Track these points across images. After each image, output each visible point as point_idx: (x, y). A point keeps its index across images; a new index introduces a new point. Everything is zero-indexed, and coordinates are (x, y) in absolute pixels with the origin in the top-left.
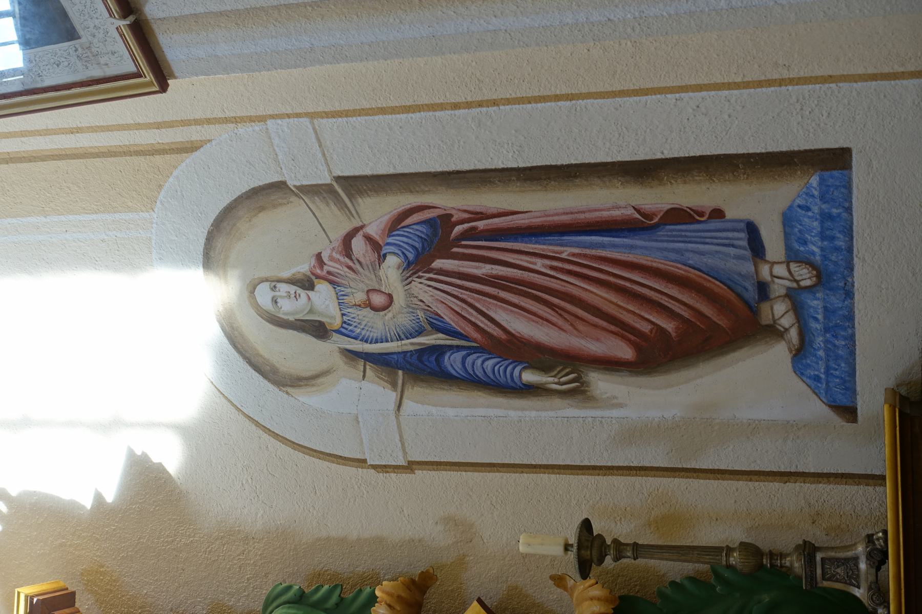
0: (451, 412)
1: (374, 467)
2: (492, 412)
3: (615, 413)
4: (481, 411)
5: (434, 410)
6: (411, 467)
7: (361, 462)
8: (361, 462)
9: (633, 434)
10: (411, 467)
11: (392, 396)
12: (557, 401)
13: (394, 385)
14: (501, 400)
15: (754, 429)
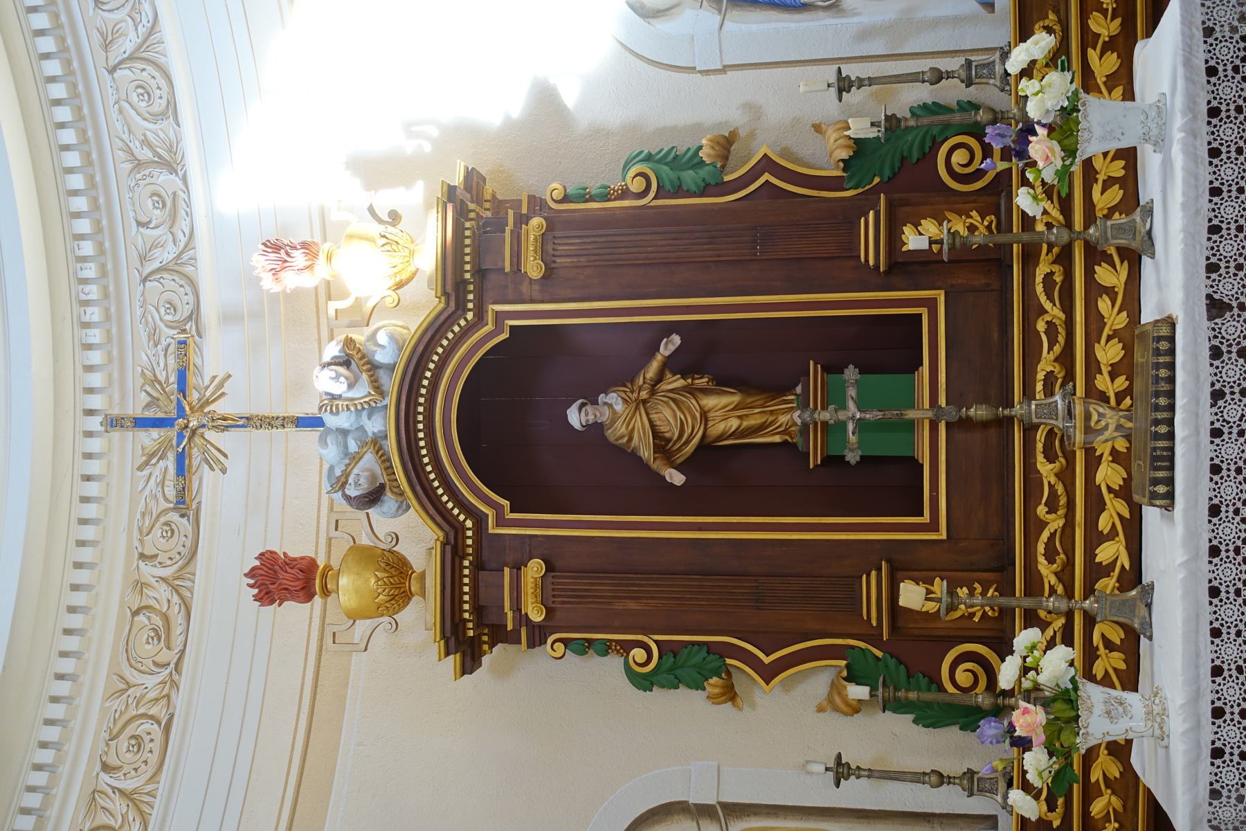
0: (754, 27)
1: (700, 72)
2: (780, 25)
3: (856, 19)
4: (773, 25)
5: (743, 27)
6: (725, 69)
7: (692, 69)
8: (692, 69)
9: (865, 34)
10: (725, 69)
11: (717, 19)
12: (821, 14)
13: (720, 11)
14: (786, 16)
15: (936, 23)
